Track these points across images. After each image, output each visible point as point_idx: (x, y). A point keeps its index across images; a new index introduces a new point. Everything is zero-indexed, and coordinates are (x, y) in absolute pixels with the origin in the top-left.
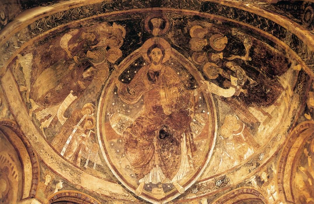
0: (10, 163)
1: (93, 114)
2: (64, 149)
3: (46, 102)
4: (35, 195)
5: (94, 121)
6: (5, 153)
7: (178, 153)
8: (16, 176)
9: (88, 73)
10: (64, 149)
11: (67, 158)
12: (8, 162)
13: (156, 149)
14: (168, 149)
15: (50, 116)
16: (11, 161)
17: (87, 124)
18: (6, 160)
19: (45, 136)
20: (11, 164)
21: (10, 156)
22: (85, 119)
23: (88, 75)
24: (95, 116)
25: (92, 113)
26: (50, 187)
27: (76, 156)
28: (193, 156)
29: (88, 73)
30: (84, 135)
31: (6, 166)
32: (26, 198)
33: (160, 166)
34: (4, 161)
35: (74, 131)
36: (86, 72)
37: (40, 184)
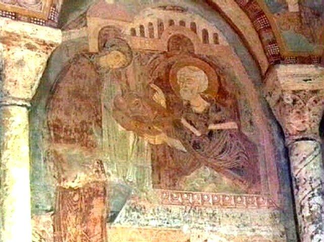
0: (177, 23)
4: (279, 54)
6: (147, 13)
8: (216, 37)
12: (171, 23)
16: (177, 17)
18: (160, 25)
20: (182, 23)
21: (164, 8)
26: (308, 11)
31: (175, 36)
32: (267, 71)
34: (156, 32)
37: (275, 20)
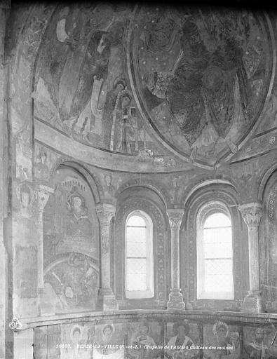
1: (126, 88)
2: (112, 142)
3: (77, 110)
5: (130, 94)
7: (230, 100)
9: (103, 44)
10: (112, 142)
11: (118, 150)
13: (205, 102)
14: (219, 99)
15: (86, 119)
17: (124, 102)
19: (91, 143)
22: (120, 98)
23: (104, 47)
24: (130, 88)
25: (125, 87)
27: (125, 143)
28: (248, 104)
29: (103, 44)
30: (126, 117)
33: (212, 122)
35: (114, 117)
36: (100, 46)
